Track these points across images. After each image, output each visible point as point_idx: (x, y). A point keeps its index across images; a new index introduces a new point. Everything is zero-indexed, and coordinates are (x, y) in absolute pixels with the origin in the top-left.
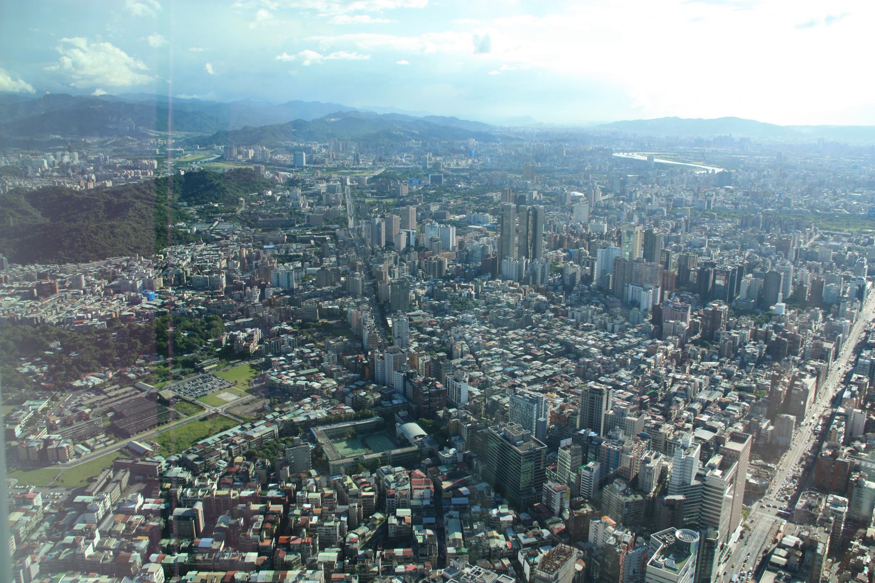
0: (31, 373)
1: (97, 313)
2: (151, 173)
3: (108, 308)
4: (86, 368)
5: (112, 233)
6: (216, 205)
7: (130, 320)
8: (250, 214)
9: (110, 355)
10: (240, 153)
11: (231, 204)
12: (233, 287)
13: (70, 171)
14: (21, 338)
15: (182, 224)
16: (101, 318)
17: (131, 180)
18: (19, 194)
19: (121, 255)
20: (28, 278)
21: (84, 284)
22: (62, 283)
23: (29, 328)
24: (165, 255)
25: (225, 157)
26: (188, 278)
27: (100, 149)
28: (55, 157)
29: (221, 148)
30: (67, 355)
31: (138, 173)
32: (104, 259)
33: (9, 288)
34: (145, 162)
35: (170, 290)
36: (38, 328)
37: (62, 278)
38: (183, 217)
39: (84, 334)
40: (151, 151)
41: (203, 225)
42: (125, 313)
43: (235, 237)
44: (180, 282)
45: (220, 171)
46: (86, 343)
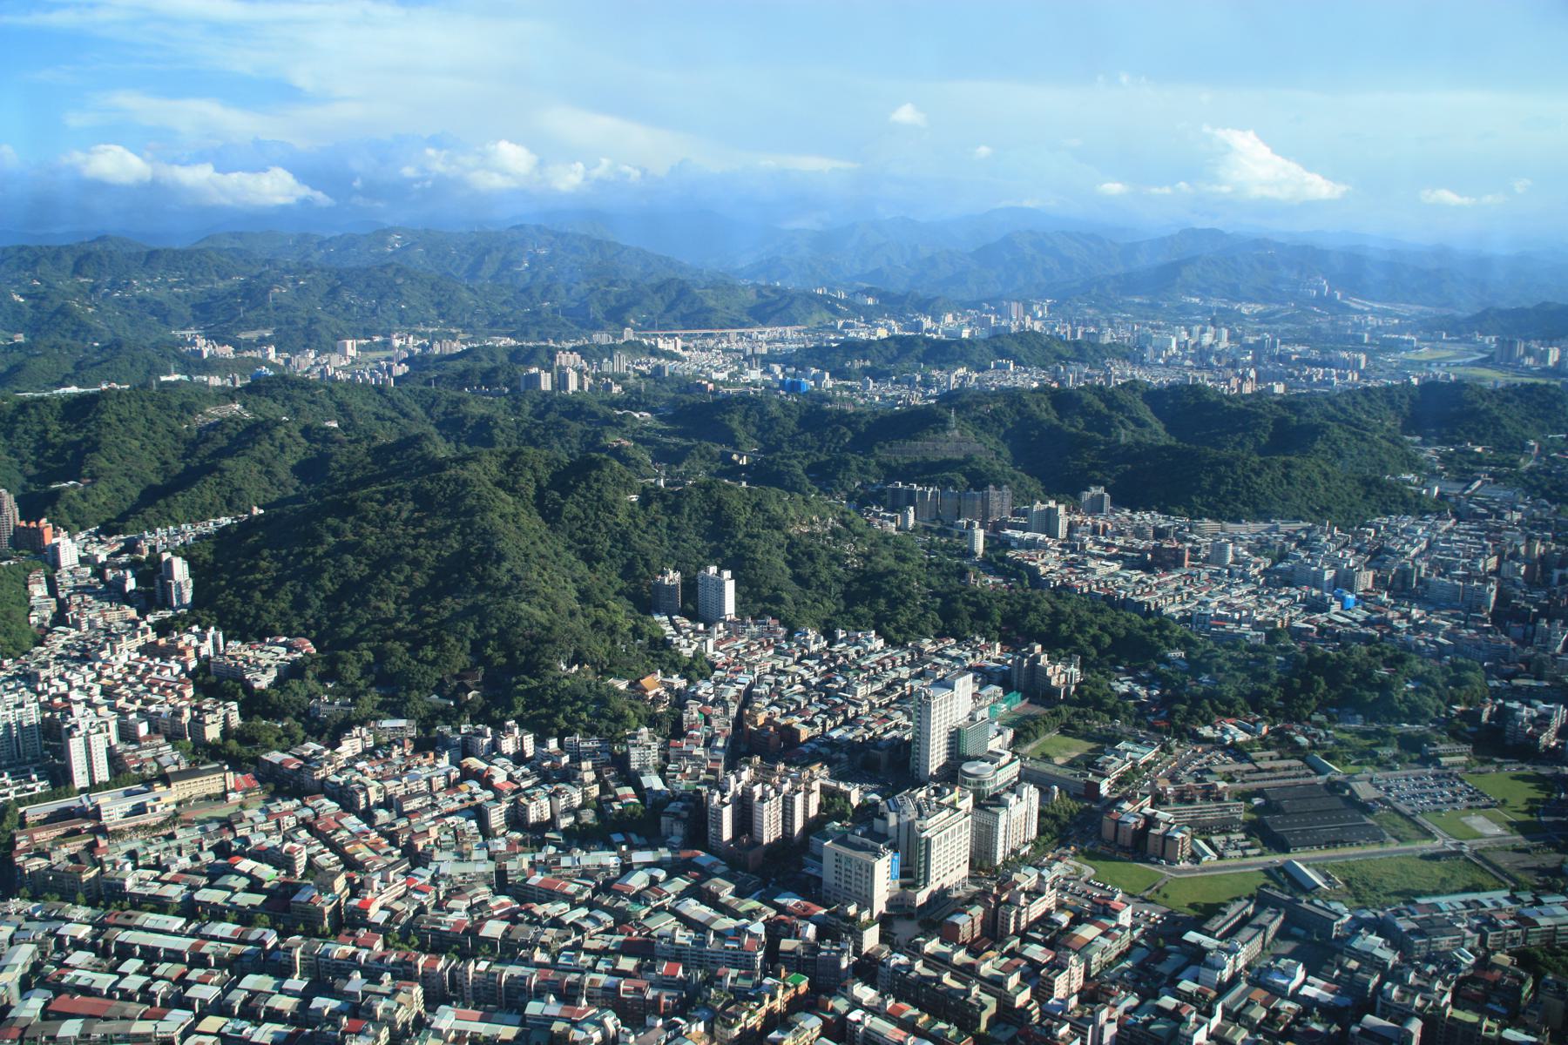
0: (1131, 695)
1: (1250, 615)
2: (1353, 377)
3: (1269, 609)
4: (1224, 708)
5: (1286, 476)
6: (1479, 449)
7: (1306, 639)
8: (1548, 473)
9: (1269, 694)
10: (1528, 352)
11: (1510, 449)
12: (1506, 613)
13: (1212, 359)
14: (1123, 633)
15: (1410, 477)
16: (1257, 626)
17: (1316, 385)
18: (1135, 390)
19: (1297, 518)
20: (1139, 533)
21: (1230, 559)
22: (1194, 551)
23: (1136, 617)
24: (1377, 531)
25: (1497, 358)
26: (1420, 581)
27: (1263, 326)
28: (1190, 334)
29: (1490, 341)
30: (1196, 677)
31: (1330, 375)
32: (1267, 521)
33: (1108, 546)
34: (1344, 355)
35: (1384, 597)
36: (1151, 621)
37: (1194, 541)
38: (1412, 464)
39: (1226, 647)
40: (1354, 337)
41: (1450, 485)
42: (1298, 624)
43: (1517, 516)
44: (1402, 587)
45: (1489, 385)
46: (1229, 665)
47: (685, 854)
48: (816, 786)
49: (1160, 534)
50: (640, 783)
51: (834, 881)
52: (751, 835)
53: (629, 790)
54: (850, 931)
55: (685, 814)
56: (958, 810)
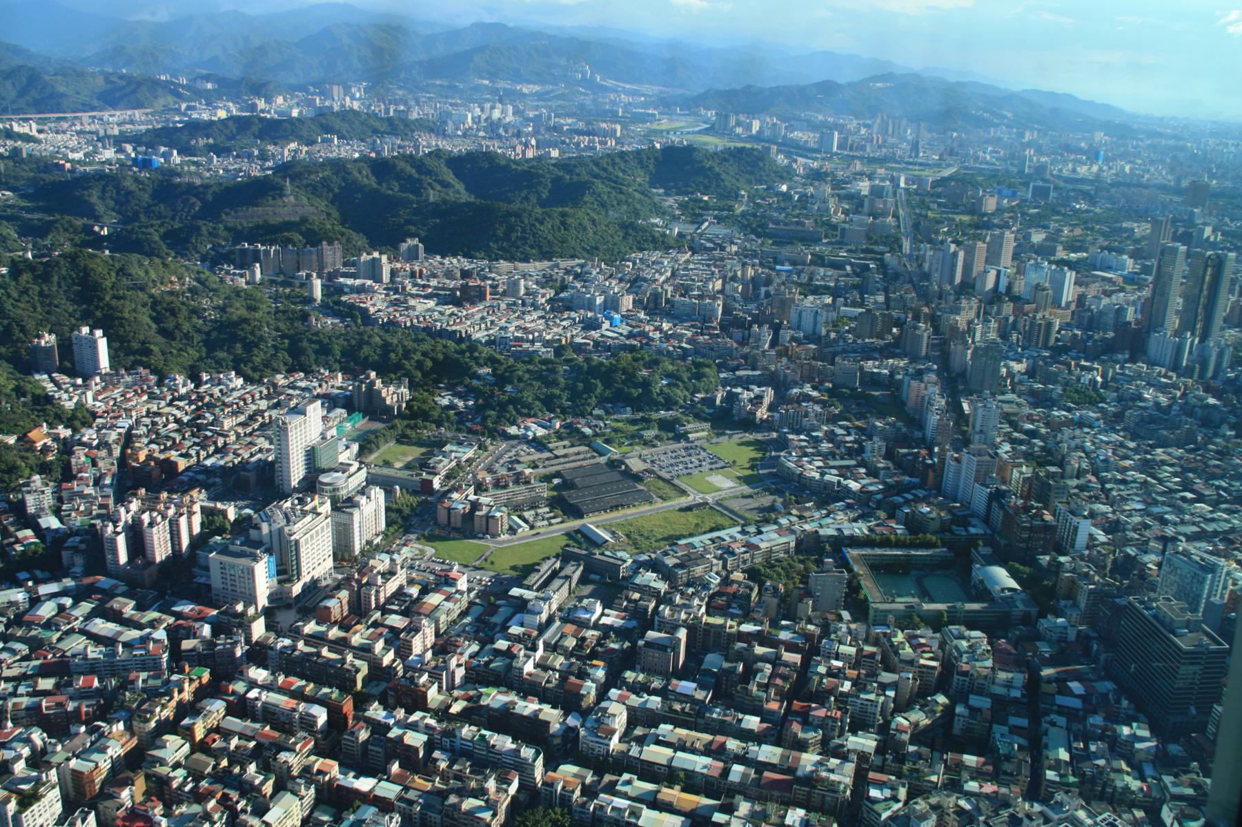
0: (452, 406)
1: (540, 336)
2: (611, 143)
3: (555, 330)
4: (526, 411)
5: (563, 223)
6: (706, 198)
7: (585, 351)
8: (755, 215)
9: (559, 397)
10: (738, 124)
11: (728, 198)
12: (731, 323)
13: (501, 131)
14: (441, 357)
15: (657, 221)
16: (547, 344)
17: (583, 150)
18: (440, 158)
19: (573, 257)
20: (449, 275)
21: (522, 291)
22: (494, 287)
23: (451, 344)
24: (634, 264)
25: (717, 127)
26: (667, 301)
27: (541, 103)
28: (482, 110)
29: (711, 114)
30: (502, 388)
31: (593, 142)
32: (550, 260)
33: (425, 286)
34: (604, 125)
35: (642, 315)
36: (463, 346)
37: (493, 279)
38: (659, 211)
39: (524, 362)
40: (611, 111)
41: (687, 226)
42: (578, 340)
43: (735, 248)
44: (654, 306)
45: (711, 148)
46: (527, 376)
47: (87, 581)
48: (197, 508)
49: (466, 274)
50: (38, 525)
51: (221, 586)
52: (144, 556)
53: (29, 532)
54: (240, 625)
55: (83, 546)
56: (319, 514)
